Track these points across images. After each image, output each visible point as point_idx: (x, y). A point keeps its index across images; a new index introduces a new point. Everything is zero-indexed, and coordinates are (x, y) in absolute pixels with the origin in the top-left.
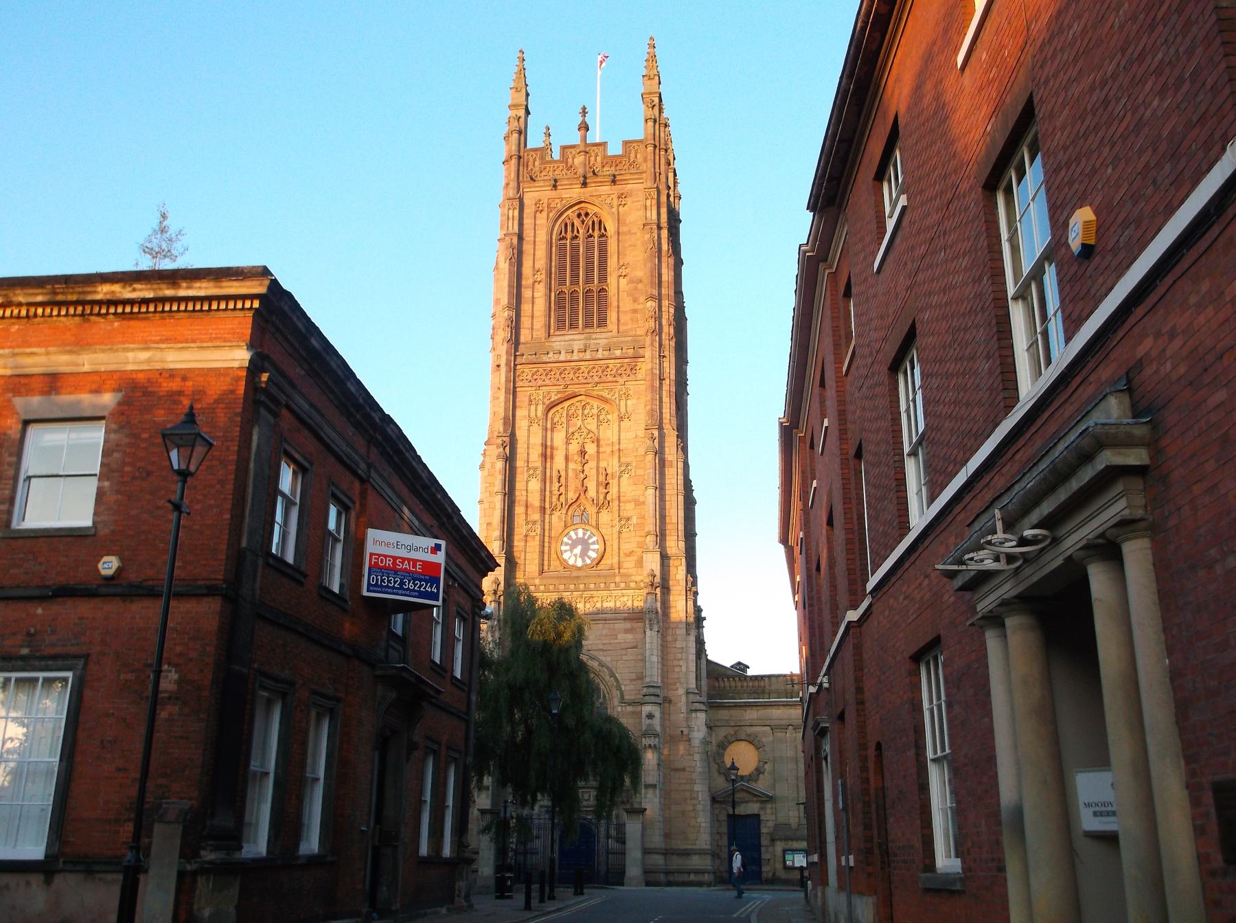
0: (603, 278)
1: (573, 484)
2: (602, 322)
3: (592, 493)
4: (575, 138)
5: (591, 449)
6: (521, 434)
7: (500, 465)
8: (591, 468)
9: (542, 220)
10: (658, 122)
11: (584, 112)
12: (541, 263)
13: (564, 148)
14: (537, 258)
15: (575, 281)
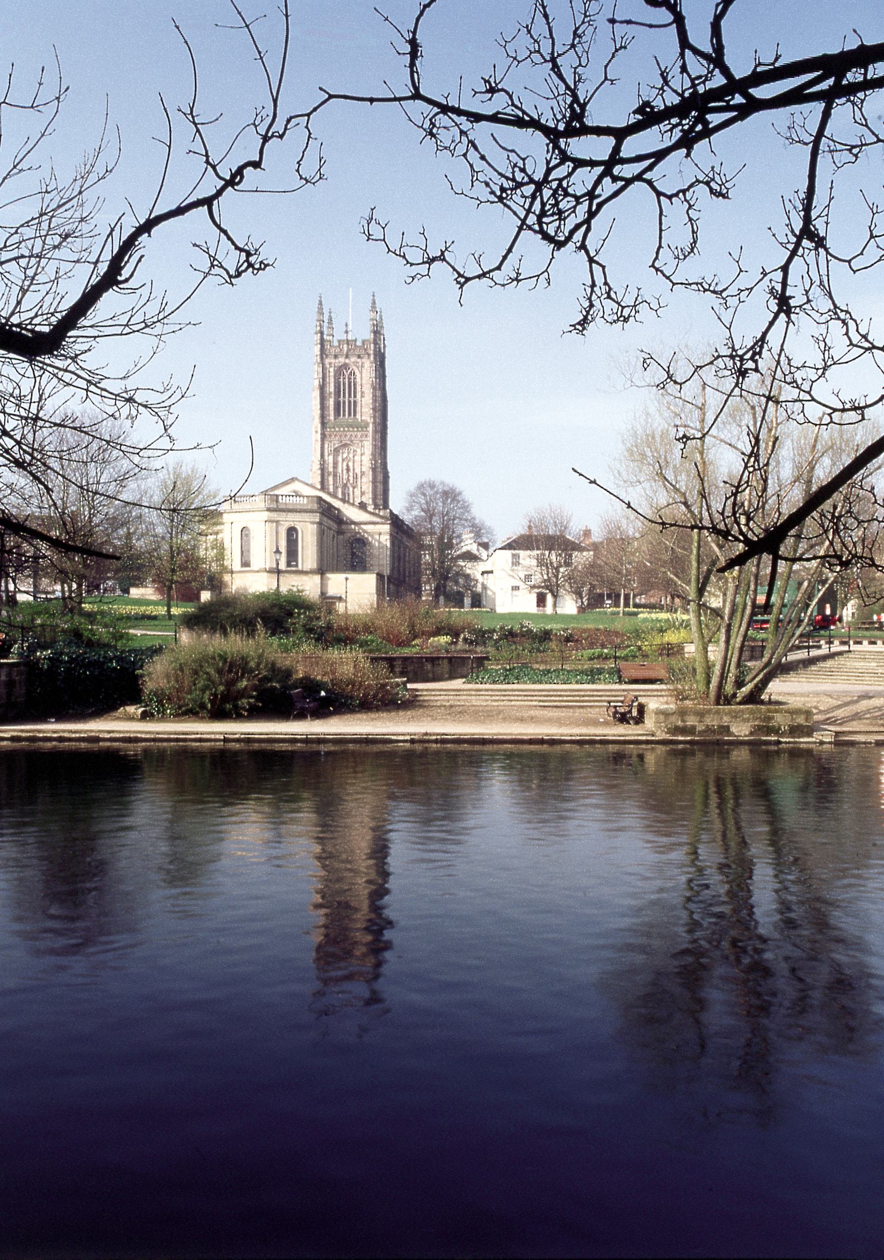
0: (355, 396)
1: (345, 477)
2: (355, 415)
3: (351, 481)
4: (344, 337)
5: (351, 464)
6: (326, 458)
7: (319, 472)
8: (351, 474)
9: (332, 370)
10: (377, 332)
11: (347, 325)
12: (332, 389)
13: (339, 341)
14: (331, 388)
15: (344, 396)
